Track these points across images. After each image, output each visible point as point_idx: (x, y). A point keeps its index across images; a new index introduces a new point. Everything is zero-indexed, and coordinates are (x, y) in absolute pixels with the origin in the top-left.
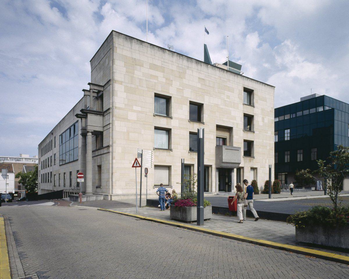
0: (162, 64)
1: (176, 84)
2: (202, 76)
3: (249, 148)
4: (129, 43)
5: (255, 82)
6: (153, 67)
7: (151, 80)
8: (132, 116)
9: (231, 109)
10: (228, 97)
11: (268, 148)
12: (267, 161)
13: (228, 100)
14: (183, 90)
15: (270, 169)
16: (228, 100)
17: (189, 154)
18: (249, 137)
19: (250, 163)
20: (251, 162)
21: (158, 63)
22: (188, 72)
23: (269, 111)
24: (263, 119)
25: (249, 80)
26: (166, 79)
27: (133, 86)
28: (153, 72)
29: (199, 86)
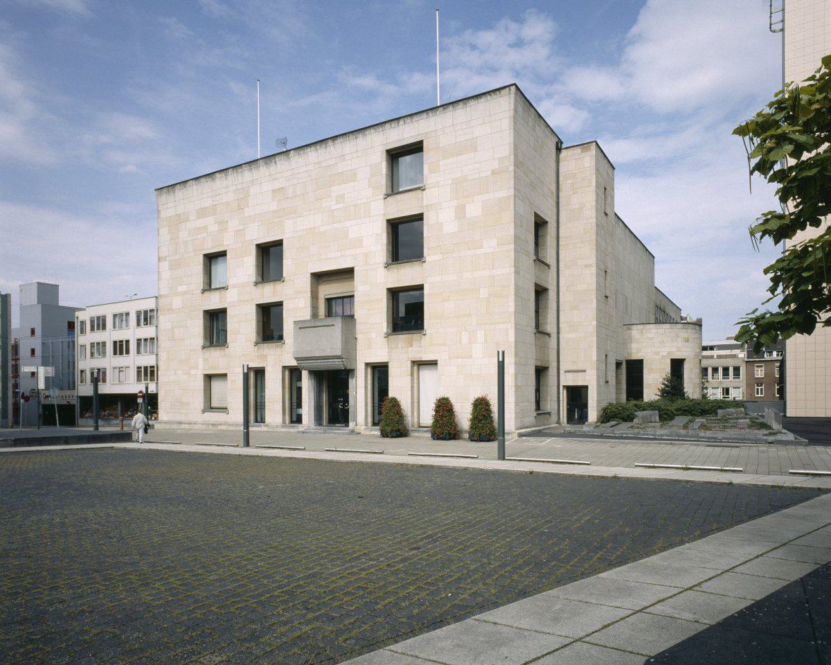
0: (213, 201)
1: (234, 224)
2: (277, 185)
3: (407, 313)
4: (172, 195)
5: (424, 115)
6: (202, 213)
7: (199, 236)
8: (177, 302)
9: (348, 224)
10: (341, 198)
11: (484, 293)
12: (480, 335)
13: (341, 205)
14: (244, 229)
15: (501, 366)
16: (341, 205)
17: (256, 347)
18: (405, 275)
19: (410, 349)
20: (411, 346)
21: (207, 203)
22: (253, 190)
23: (489, 173)
24: (460, 211)
25: (401, 122)
26: (219, 223)
27: (177, 257)
28: (201, 223)
29: (274, 206)
